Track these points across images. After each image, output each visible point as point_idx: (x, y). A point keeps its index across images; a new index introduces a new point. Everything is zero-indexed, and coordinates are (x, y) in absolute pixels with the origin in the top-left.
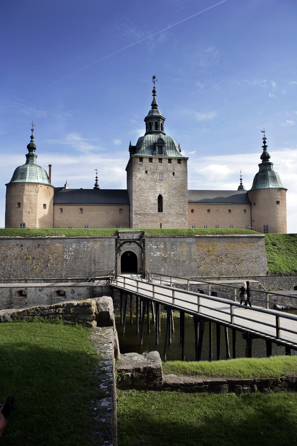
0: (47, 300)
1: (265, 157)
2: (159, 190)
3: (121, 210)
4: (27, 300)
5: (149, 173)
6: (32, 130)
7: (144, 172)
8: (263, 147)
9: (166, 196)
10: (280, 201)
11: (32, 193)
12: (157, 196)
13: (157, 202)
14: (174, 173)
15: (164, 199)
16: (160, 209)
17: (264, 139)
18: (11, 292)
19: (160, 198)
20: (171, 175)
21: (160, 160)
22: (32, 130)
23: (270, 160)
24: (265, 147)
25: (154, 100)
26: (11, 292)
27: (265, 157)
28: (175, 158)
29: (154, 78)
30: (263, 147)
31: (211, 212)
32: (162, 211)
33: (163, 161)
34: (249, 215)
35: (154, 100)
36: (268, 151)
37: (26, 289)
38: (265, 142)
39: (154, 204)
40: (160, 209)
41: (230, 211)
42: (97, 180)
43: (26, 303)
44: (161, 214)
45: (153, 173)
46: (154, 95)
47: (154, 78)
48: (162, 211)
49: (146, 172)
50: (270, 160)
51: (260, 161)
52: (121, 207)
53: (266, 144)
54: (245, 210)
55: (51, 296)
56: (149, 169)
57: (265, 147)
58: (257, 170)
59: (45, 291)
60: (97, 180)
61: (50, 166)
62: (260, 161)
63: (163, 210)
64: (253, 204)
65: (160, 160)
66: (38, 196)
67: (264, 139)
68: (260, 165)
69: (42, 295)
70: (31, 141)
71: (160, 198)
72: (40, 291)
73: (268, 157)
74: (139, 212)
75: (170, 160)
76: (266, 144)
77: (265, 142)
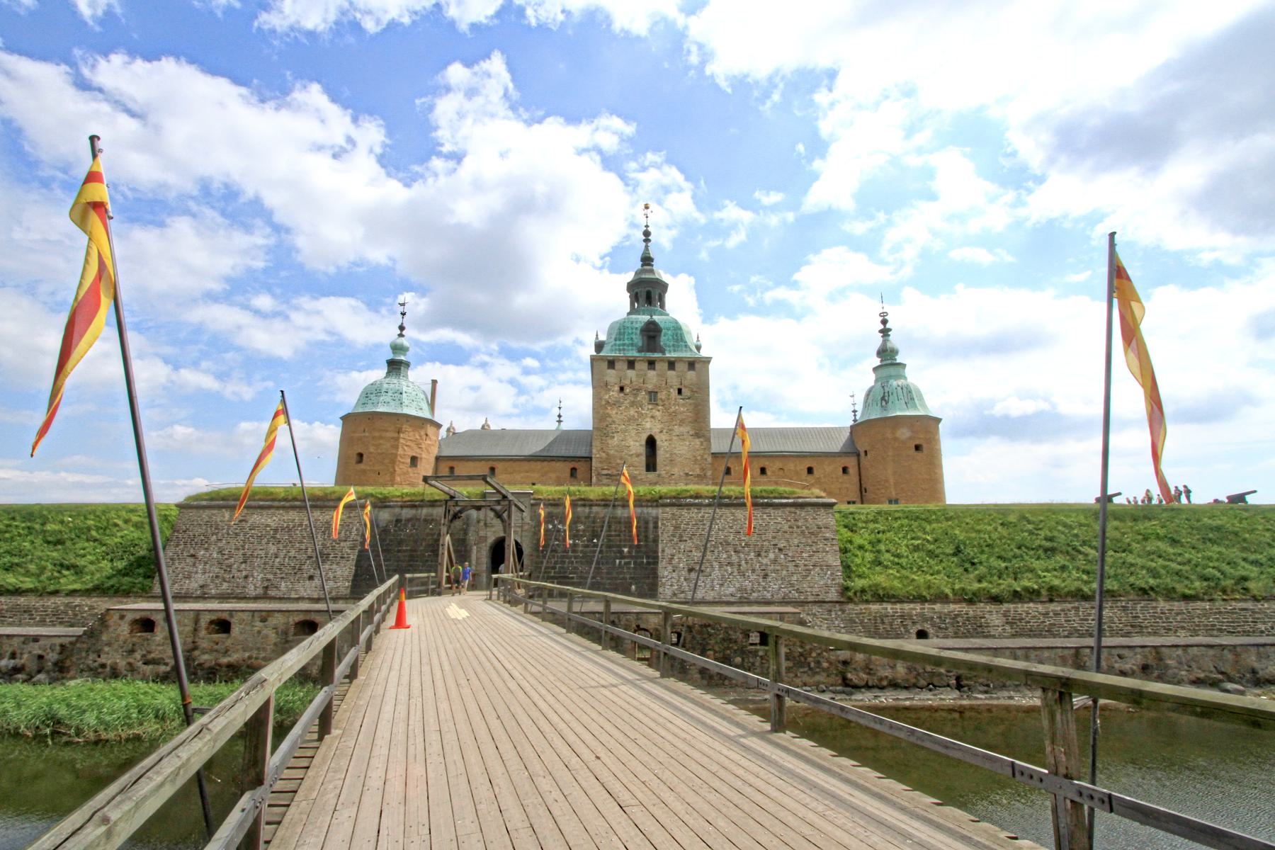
0: (275, 644)
1: (887, 355)
2: (648, 425)
3: (573, 470)
4: (229, 643)
5: (627, 390)
6: (403, 314)
7: (617, 388)
8: (881, 331)
9: (664, 438)
10: (925, 446)
11: (388, 435)
12: (644, 437)
13: (642, 450)
14: (680, 391)
15: (659, 443)
16: (651, 466)
18: (197, 621)
19: (651, 443)
20: (674, 392)
21: (651, 364)
22: (403, 314)
23: (899, 359)
24: (885, 332)
25: (647, 247)
26: (197, 621)
27: (887, 355)
28: (680, 359)
29: (647, 207)
30: (881, 331)
31: (768, 472)
32: (655, 470)
33: (658, 366)
34: (856, 479)
35: (647, 247)
36: (894, 340)
37: (232, 616)
38: (884, 322)
39: (638, 455)
40: (651, 466)
41: (810, 470)
42: (559, 422)
43: (227, 651)
44: (651, 475)
45: (638, 390)
46: (647, 241)
47: (647, 207)
48: (655, 470)
49: (622, 389)
50: (899, 359)
51: (877, 362)
52: (572, 465)
53: (888, 326)
54: (845, 470)
55: (286, 633)
56: (628, 382)
57: (885, 332)
58: (870, 380)
59: (273, 621)
60: (559, 422)
61: (434, 382)
62: (877, 362)
63: (658, 467)
65: (651, 364)
66: (402, 441)
68: (875, 369)
69: (265, 632)
70: (401, 335)
71: (651, 443)
72: (264, 620)
73: (894, 352)
74: (605, 472)
75: (672, 365)
76: (888, 326)
77: (884, 322)
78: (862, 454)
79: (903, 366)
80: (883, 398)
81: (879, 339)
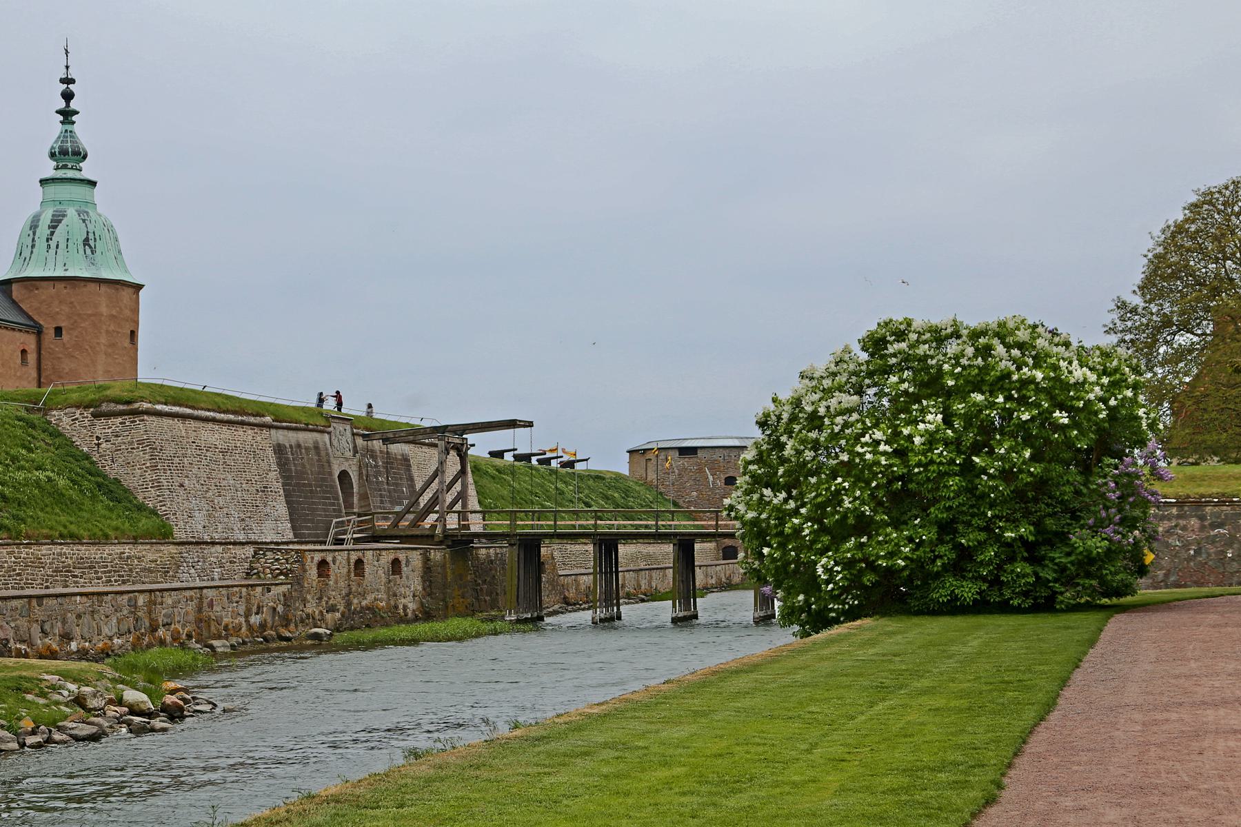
1: (68, 154)
17: (68, 81)
18: (348, 559)
23: (87, 170)
24: (67, 115)
26: (348, 559)
27: (68, 154)
38: (68, 96)
50: (87, 170)
51: (49, 169)
53: (74, 105)
57: (67, 115)
62: (49, 169)
64: (50, 333)
67: (68, 81)
68: (43, 182)
77: (68, 96)
78: (50, 333)
79: (93, 184)
80: (86, 242)
81: (56, 125)
